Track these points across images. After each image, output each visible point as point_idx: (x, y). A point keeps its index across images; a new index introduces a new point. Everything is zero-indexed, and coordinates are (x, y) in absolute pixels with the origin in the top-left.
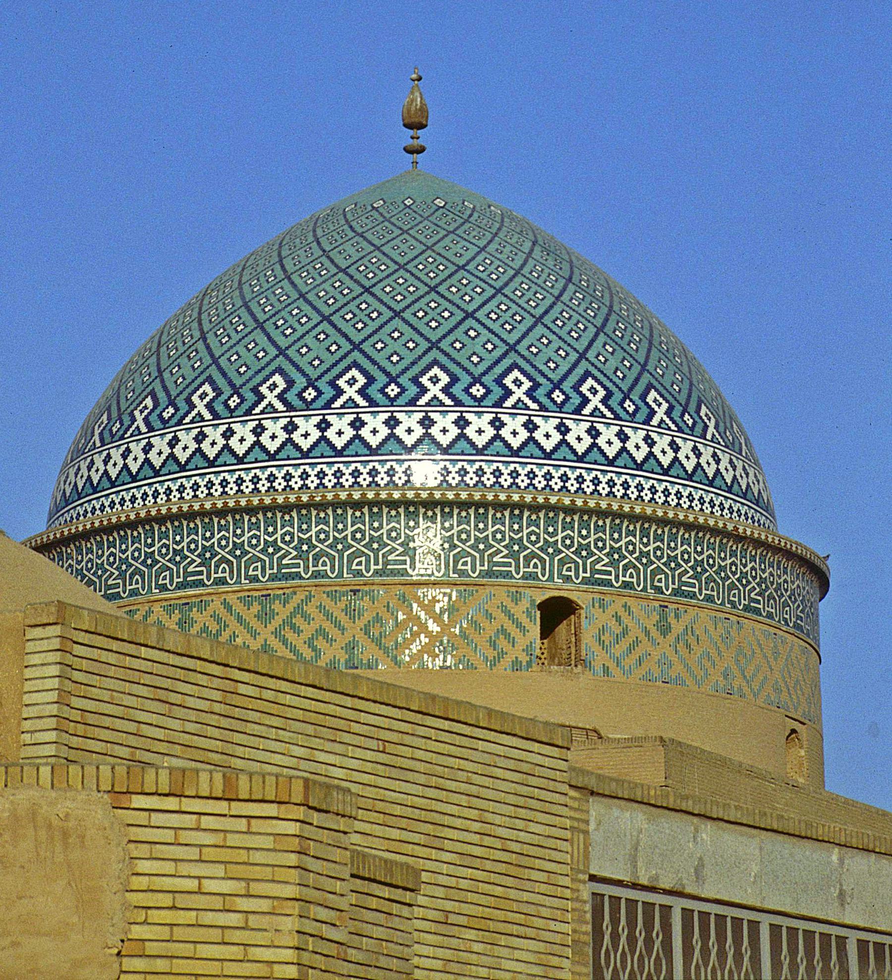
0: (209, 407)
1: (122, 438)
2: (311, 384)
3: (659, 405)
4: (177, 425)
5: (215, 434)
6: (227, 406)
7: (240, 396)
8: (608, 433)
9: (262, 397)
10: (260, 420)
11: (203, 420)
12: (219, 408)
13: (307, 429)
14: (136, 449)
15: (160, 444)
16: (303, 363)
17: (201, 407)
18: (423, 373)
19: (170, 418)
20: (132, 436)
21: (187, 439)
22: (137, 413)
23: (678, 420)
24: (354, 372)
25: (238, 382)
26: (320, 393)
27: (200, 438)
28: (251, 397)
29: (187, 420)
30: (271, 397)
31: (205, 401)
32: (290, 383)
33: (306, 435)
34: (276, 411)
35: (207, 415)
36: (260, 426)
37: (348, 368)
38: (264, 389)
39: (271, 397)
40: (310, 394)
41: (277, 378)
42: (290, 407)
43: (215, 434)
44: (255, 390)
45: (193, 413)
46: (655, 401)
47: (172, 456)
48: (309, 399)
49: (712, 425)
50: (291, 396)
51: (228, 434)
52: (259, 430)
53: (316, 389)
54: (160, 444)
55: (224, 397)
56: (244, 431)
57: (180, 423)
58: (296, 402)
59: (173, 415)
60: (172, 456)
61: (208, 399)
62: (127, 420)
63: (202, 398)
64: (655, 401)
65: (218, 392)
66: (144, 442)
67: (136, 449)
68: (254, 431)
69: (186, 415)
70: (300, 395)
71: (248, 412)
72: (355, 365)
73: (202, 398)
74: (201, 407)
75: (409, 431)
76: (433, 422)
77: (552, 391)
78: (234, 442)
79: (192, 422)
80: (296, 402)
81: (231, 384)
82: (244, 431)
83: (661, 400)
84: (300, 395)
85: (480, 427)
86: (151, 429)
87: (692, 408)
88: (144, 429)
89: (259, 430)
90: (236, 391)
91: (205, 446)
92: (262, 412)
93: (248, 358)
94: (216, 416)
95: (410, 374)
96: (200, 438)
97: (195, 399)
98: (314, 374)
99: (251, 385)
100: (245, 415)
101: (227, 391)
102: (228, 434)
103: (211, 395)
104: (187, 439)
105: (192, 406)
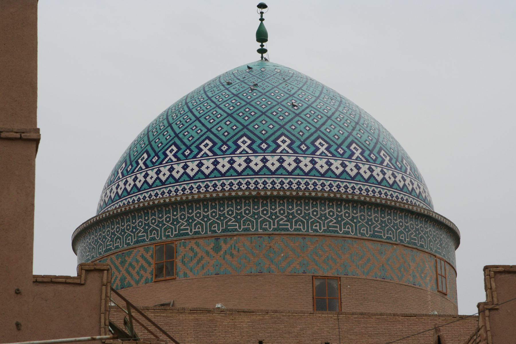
0: (175, 156)
2: (225, 143)
4: (159, 164)
5: (178, 168)
6: (184, 155)
7: (190, 150)
9: (201, 150)
10: (200, 160)
11: (172, 161)
12: (179, 155)
13: (224, 164)
15: (152, 173)
16: (220, 135)
17: (170, 155)
19: (156, 161)
21: (165, 170)
24: (245, 138)
25: (188, 143)
27: (171, 170)
28: (196, 151)
29: (164, 162)
30: (205, 150)
32: (215, 144)
34: (208, 156)
35: (174, 159)
38: (202, 146)
39: (205, 150)
41: (207, 141)
42: (215, 154)
43: (178, 168)
44: (198, 147)
47: (158, 178)
48: (224, 150)
50: (215, 149)
51: (185, 167)
52: (200, 165)
53: (227, 145)
54: (152, 173)
56: (193, 165)
57: (161, 163)
58: (219, 152)
59: (157, 160)
60: (158, 178)
61: (174, 152)
63: (171, 152)
65: (179, 149)
66: (144, 173)
67: (141, 177)
69: (163, 160)
70: (220, 149)
71: (195, 157)
72: (245, 135)
73: (171, 151)
74: (170, 155)
79: (166, 163)
80: (219, 152)
81: (184, 144)
82: (193, 165)
84: (220, 149)
86: (147, 166)
89: (200, 165)
90: (188, 148)
91: (174, 173)
92: (201, 157)
93: (193, 133)
94: (179, 159)
95: (273, 138)
96: (171, 170)
97: (168, 152)
98: (225, 139)
99: (195, 145)
101: (183, 147)
102: (185, 167)
103: (175, 150)
104: (165, 170)
105: (166, 156)
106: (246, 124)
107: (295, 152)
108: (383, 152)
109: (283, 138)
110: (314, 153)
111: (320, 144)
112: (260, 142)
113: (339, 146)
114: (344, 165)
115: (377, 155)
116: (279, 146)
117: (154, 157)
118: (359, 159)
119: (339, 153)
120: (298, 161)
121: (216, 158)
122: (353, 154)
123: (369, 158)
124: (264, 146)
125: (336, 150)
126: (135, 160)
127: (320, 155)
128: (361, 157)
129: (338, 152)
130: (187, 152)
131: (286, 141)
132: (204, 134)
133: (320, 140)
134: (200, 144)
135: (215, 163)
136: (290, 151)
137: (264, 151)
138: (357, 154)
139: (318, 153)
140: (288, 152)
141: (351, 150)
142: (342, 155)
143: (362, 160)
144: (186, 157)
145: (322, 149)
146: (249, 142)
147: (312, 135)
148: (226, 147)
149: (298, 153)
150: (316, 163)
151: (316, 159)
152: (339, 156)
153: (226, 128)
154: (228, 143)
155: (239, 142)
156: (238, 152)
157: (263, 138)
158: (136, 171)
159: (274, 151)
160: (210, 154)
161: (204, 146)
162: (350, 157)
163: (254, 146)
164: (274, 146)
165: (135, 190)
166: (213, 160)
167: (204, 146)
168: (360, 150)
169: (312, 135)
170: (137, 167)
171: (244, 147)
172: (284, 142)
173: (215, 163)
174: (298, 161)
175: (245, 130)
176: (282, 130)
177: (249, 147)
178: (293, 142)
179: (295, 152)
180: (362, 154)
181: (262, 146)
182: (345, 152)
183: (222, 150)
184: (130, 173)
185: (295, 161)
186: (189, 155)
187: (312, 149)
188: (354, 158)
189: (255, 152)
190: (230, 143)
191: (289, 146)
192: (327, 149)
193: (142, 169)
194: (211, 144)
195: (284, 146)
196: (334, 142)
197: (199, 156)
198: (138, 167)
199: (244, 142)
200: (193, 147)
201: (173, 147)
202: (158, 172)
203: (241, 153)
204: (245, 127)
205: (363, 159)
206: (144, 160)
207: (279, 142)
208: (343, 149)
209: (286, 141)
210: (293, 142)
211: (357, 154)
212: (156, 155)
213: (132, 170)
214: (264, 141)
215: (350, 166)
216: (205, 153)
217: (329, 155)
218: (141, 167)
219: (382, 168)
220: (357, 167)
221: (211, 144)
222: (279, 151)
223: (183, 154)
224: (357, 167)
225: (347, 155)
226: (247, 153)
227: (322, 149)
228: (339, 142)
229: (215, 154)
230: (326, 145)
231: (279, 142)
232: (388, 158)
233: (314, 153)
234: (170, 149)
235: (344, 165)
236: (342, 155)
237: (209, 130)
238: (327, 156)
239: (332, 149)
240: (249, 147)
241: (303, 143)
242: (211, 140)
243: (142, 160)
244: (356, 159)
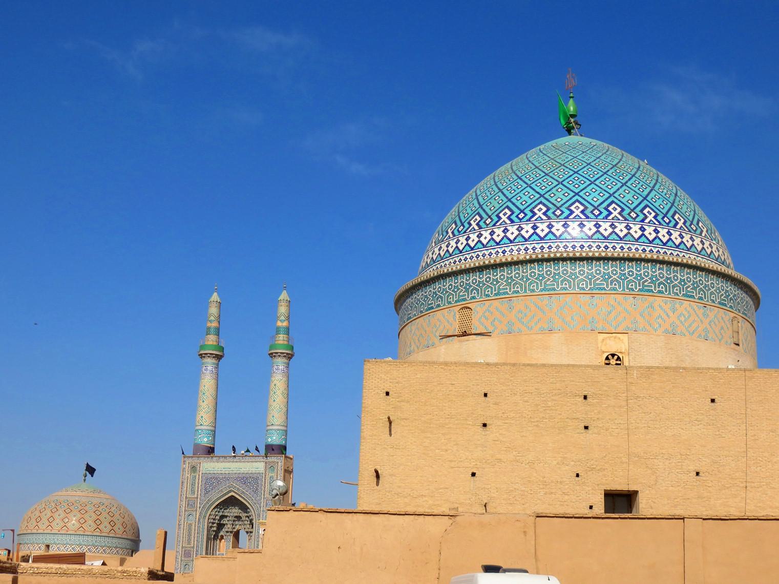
0: (509, 218)
1: (465, 232)
3: (680, 220)
4: (493, 226)
5: (513, 230)
7: (524, 213)
8: (663, 232)
9: (535, 214)
11: (506, 223)
12: (513, 217)
14: (474, 237)
17: (504, 218)
18: (617, 204)
19: (489, 223)
20: (470, 231)
21: (499, 231)
22: (472, 222)
23: (689, 227)
24: (577, 204)
26: (526, 215)
27: (505, 231)
29: (498, 224)
30: (540, 214)
31: (506, 216)
33: (527, 232)
34: (542, 220)
36: (535, 225)
37: (539, 204)
39: (540, 214)
40: (558, 213)
42: (549, 218)
45: (501, 221)
46: (678, 218)
49: (705, 230)
50: (549, 213)
51: (520, 229)
52: (535, 227)
54: (486, 234)
55: (515, 214)
56: (527, 229)
57: (494, 225)
59: (491, 222)
61: (507, 215)
62: (467, 225)
64: (678, 218)
68: (503, 231)
70: (554, 213)
73: (505, 214)
74: (504, 218)
75: (621, 230)
76: (600, 226)
77: (630, 213)
78: (495, 237)
79: (500, 224)
83: (681, 218)
85: (635, 230)
86: (480, 228)
87: (695, 222)
88: (476, 228)
89: (535, 227)
90: (522, 211)
92: (536, 220)
94: (512, 221)
96: (505, 231)
98: (558, 205)
100: (527, 221)
101: (517, 212)
104: (499, 231)
105: (500, 218)
106: (577, 191)
107: (626, 219)
108: (700, 224)
109: (614, 205)
110: (643, 221)
111: (648, 212)
112: (593, 208)
113: (665, 216)
114: (669, 233)
115: (697, 226)
116: (610, 213)
117: (487, 219)
118: (682, 228)
119: (666, 222)
120: (628, 228)
121: (550, 222)
122: (677, 223)
123: (690, 229)
124: (596, 212)
125: (663, 218)
126: (467, 221)
127: (649, 223)
128: (684, 227)
129: (664, 221)
130: (521, 216)
131: (616, 209)
132: (537, 199)
133: (648, 209)
134: (534, 208)
135: (550, 226)
136: (621, 218)
137: (597, 216)
138: (681, 223)
139: (647, 221)
140: (619, 219)
141: (675, 219)
142: (668, 224)
143: (685, 230)
144: (520, 219)
145: (651, 217)
146: (582, 208)
147: (640, 204)
148: (560, 212)
149: (628, 220)
150: (645, 230)
151: (645, 227)
152: (665, 224)
153: (560, 195)
154: (561, 209)
155: (572, 208)
156: (571, 217)
157: (596, 204)
158: (468, 231)
159: (606, 217)
160: (544, 217)
161: (538, 210)
162: (675, 226)
163: (587, 212)
164: (605, 213)
165: (457, 252)
166: (548, 223)
167: (538, 210)
168: (682, 221)
169: (640, 204)
170: (469, 227)
171: (577, 212)
172: (615, 209)
173: (550, 226)
174: (628, 228)
175: (577, 197)
176: (612, 199)
177: (582, 212)
178: (623, 210)
179: (626, 219)
180: (684, 223)
181: (594, 212)
182: (670, 221)
183: (556, 215)
184: (462, 232)
185: (626, 227)
186: (523, 218)
187: (641, 216)
188: (678, 227)
189: (587, 217)
190: (563, 209)
191: (620, 213)
192: (655, 217)
193: (475, 230)
194: (544, 209)
195: (615, 213)
196: (660, 211)
197: (533, 219)
198: (471, 228)
199: (577, 208)
200: (527, 211)
201: (506, 210)
202: (492, 233)
203: (573, 218)
204: (577, 194)
205: (685, 228)
206: (477, 221)
207: (610, 208)
208: (668, 219)
209: (616, 209)
210: (623, 210)
211: (681, 223)
212: (490, 217)
213: (464, 230)
214: (596, 208)
215: (675, 235)
216: (540, 217)
217: (657, 223)
218: (473, 228)
219: (702, 238)
220: (681, 237)
221: (544, 209)
222: (610, 217)
223: (517, 216)
224: (681, 237)
225: (672, 224)
226: (581, 218)
227: (651, 217)
228: (664, 211)
229: (549, 218)
230: (653, 214)
231: (610, 208)
232: (705, 229)
233: (643, 221)
234: (504, 212)
235: (669, 233)
236: (668, 224)
237: (542, 196)
238: (655, 224)
239: (659, 218)
240: (582, 212)
241: (632, 210)
242: (544, 205)
243: (474, 222)
244: (680, 229)
